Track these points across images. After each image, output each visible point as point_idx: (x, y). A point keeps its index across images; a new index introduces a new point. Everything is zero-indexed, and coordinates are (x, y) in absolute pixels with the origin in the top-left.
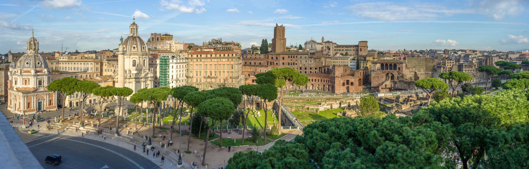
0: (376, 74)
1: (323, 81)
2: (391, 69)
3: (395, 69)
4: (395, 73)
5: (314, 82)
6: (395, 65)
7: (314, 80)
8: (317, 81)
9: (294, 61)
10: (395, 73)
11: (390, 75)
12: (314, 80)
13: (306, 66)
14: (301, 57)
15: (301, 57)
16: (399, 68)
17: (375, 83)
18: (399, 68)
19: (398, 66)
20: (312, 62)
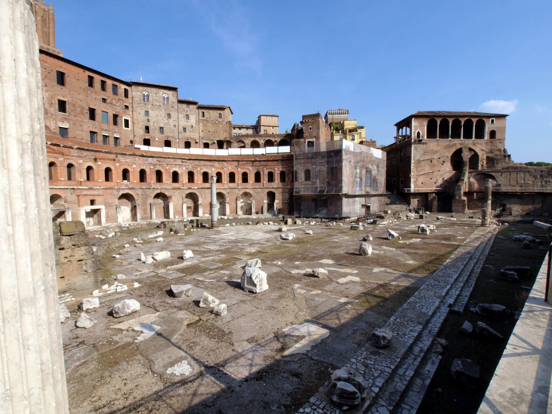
0: (425, 153)
1: (264, 178)
2: (468, 136)
3: (480, 135)
4: (481, 147)
5: (225, 186)
6: (481, 126)
7: (225, 178)
8: (238, 178)
9: (119, 109)
10: (481, 147)
11: (466, 156)
12: (225, 178)
13: (168, 134)
14: (146, 98)
15: (146, 98)
16: (493, 134)
17: (421, 179)
18: (493, 134)
19: (488, 127)
20: (193, 120)
